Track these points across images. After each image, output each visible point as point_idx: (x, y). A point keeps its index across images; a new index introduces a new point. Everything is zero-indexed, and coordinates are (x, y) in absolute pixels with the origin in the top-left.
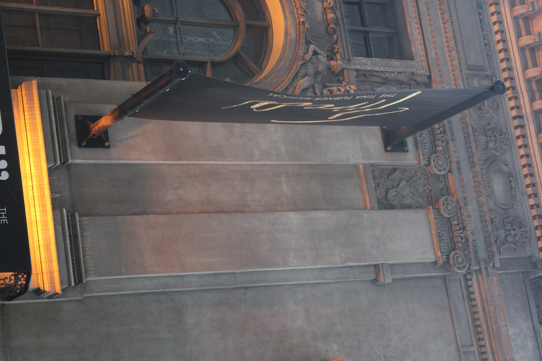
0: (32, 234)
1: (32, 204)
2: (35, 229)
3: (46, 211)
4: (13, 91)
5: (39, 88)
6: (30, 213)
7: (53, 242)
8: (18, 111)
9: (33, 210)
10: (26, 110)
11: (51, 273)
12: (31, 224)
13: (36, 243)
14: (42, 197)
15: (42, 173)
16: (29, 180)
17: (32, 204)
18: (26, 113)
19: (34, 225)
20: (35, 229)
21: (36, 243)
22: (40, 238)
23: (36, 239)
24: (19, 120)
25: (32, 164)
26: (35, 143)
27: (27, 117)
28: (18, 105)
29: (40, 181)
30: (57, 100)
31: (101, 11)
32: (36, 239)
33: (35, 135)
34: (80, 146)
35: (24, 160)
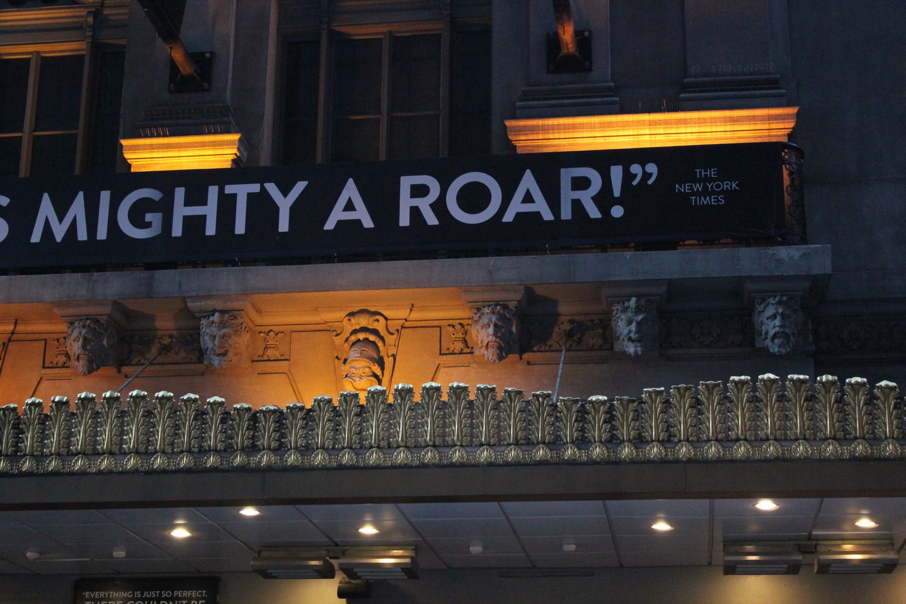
0: (716, 139)
1: (674, 137)
2: (709, 135)
3: (685, 119)
4: (519, 151)
5: (514, 117)
6: (686, 141)
7: (728, 113)
8: (546, 146)
9: (683, 137)
10: (546, 136)
11: (770, 118)
12: (701, 139)
13: (729, 135)
14: (667, 123)
15: (633, 121)
16: (641, 138)
17: (674, 137)
18: (551, 136)
19: (703, 136)
20: (709, 135)
21: (729, 135)
22: (722, 129)
23: (723, 135)
24: (560, 145)
25: (621, 133)
26: (592, 127)
27: (556, 136)
28: (538, 146)
29: (644, 125)
30: (526, 96)
31: (385, 29)
32: (723, 135)
33: (581, 127)
34: (590, 70)
35: (614, 143)
